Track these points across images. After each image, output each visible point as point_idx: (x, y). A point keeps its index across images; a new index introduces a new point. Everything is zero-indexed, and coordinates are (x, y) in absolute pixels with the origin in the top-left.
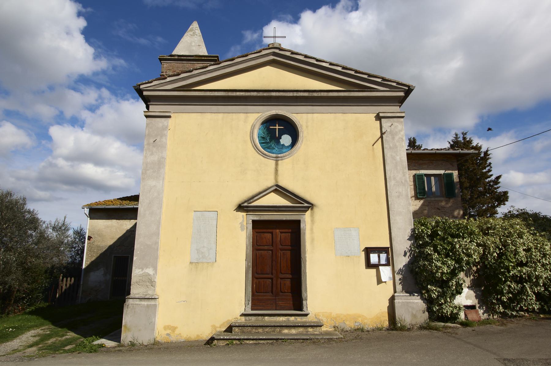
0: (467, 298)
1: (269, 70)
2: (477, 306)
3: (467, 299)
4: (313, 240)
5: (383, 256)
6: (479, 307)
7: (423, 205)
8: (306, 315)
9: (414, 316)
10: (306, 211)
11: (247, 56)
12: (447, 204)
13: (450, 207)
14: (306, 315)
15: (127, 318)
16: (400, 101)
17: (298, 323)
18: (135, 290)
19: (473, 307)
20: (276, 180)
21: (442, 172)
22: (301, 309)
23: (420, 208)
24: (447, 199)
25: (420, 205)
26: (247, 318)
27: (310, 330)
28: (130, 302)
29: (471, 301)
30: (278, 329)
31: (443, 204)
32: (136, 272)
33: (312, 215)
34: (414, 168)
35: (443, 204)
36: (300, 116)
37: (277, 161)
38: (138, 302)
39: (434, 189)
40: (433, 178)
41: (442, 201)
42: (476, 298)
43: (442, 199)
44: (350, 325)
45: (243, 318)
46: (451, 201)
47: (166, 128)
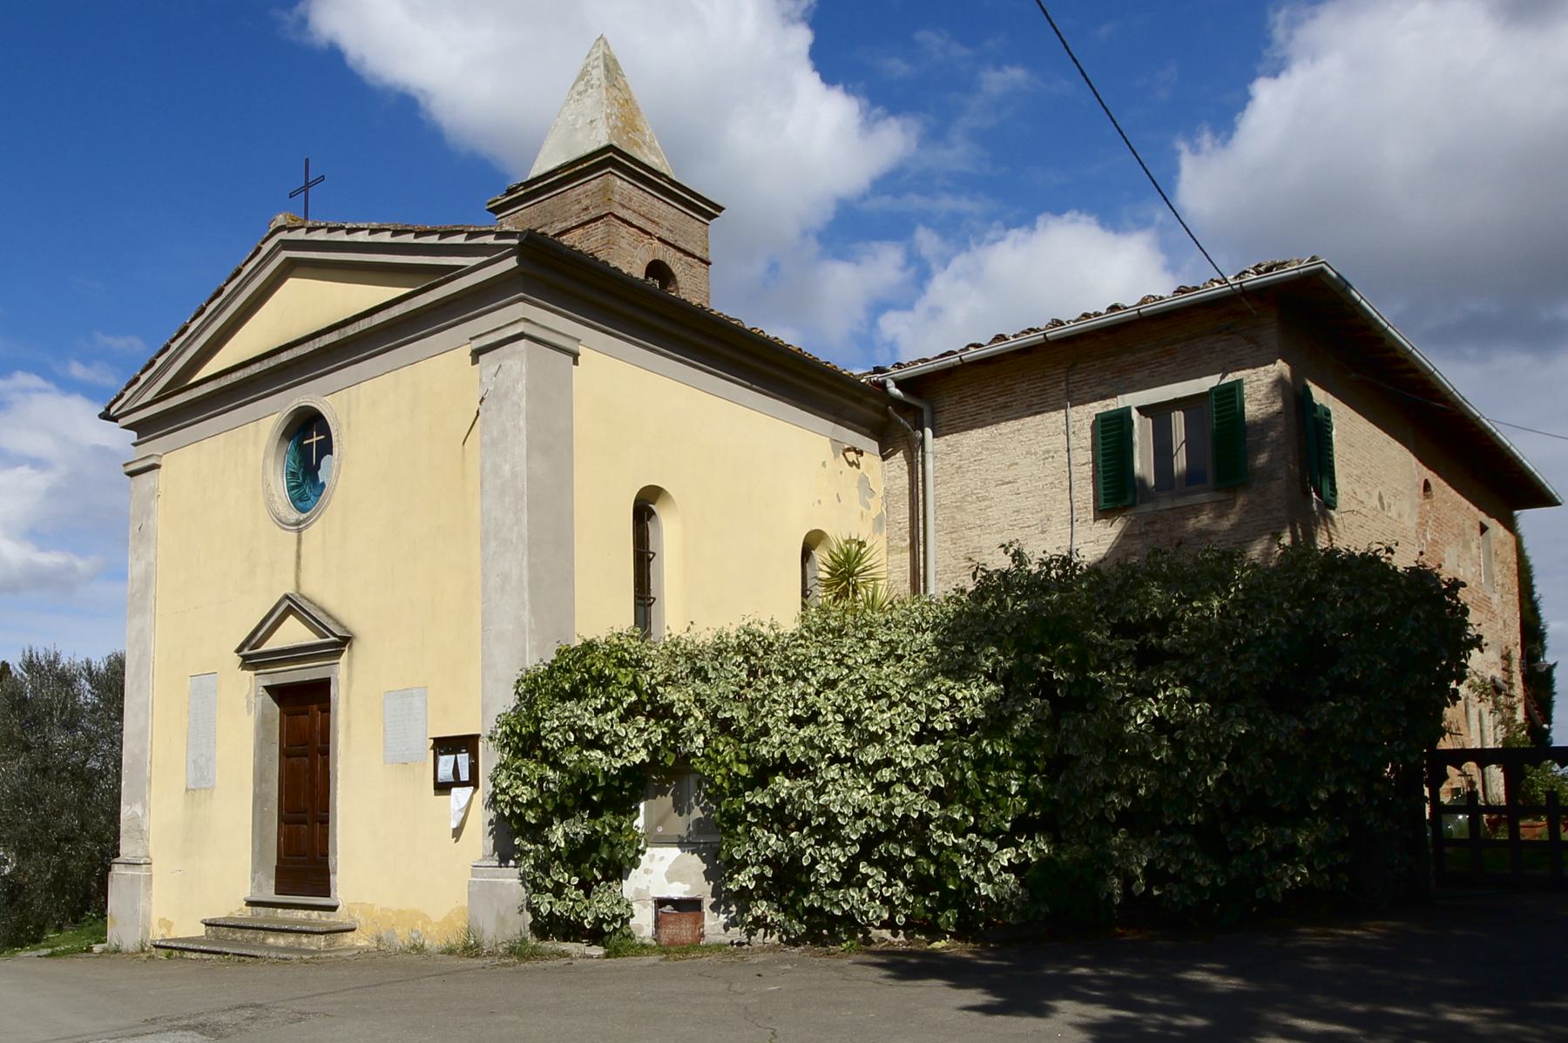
0: (672, 876)
1: (294, 287)
2: (708, 901)
3: (670, 880)
4: (348, 727)
5: (464, 759)
6: (714, 908)
7: (1125, 536)
8: (333, 908)
9: (501, 920)
10: (339, 654)
11: (239, 271)
12: (1220, 516)
13: (1234, 528)
14: (333, 908)
15: (115, 902)
16: (711, 216)
17: (324, 924)
18: (127, 848)
19: (689, 906)
20: (298, 586)
21: (1208, 382)
22: (326, 892)
23: (1116, 548)
24: (1222, 496)
25: (1113, 538)
26: (260, 909)
27: (304, 939)
28: (117, 870)
29: (687, 887)
30: (261, 934)
31: (1204, 520)
32: (125, 811)
33: (350, 664)
34: (1100, 390)
35: (1204, 520)
36: (342, 399)
37: (299, 531)
38: (130, 872)
39: (1180, 462)
40: (1178, 418)
41: (1196, 510)
42: (708, 879)
43: (1202, 497)
44: (402, 937)
45: (249, 911)
46: (1241, 501)
47: (154, 494)
